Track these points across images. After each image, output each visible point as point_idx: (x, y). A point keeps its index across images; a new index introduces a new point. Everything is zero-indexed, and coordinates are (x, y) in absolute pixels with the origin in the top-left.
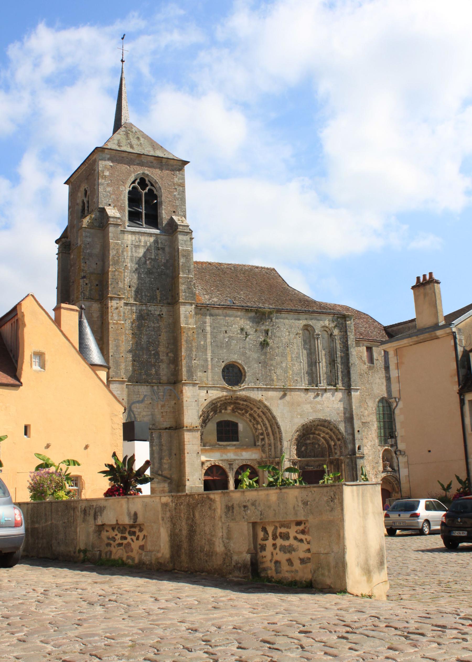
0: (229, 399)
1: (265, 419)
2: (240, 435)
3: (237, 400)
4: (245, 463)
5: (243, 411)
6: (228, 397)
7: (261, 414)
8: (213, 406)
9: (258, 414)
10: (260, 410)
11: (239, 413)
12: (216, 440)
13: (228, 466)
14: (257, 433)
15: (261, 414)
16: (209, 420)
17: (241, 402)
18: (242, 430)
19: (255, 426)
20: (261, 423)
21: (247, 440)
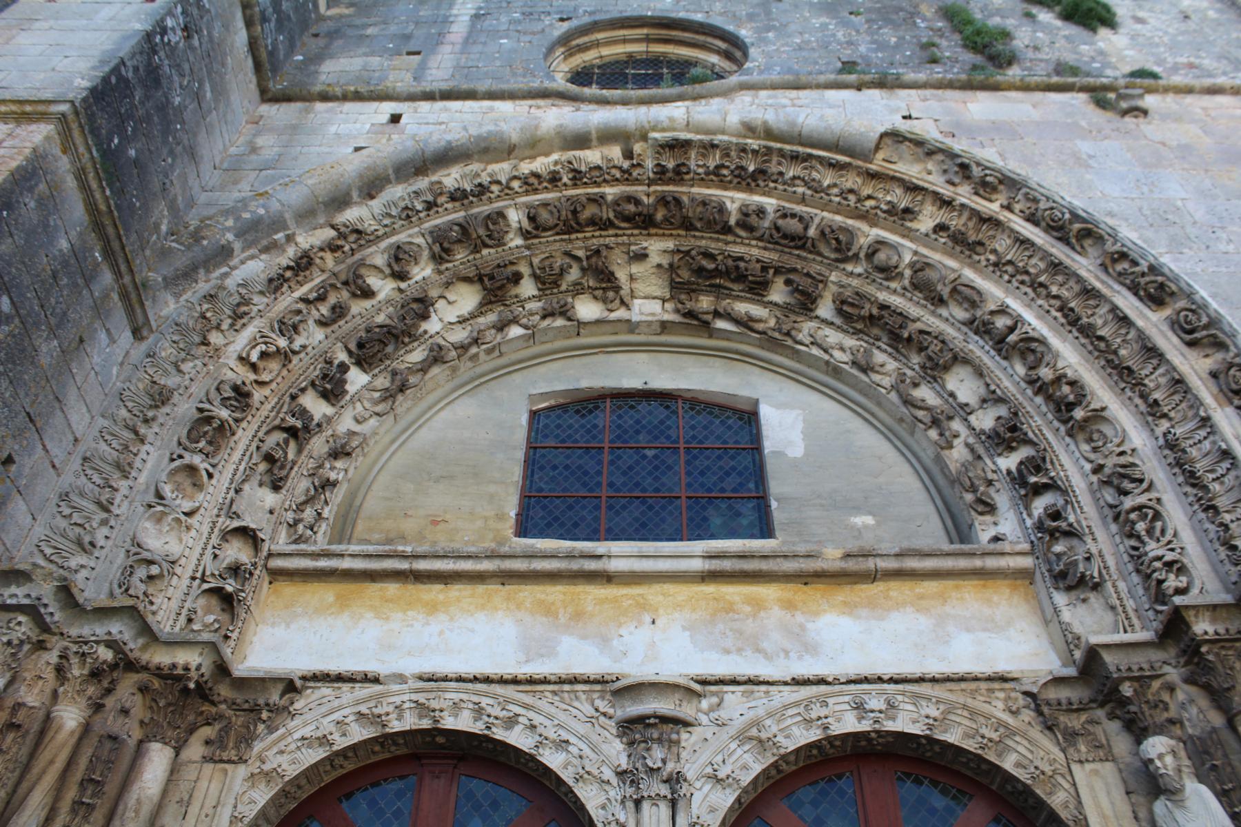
0: (598, 175)
1: (994, 291)
2: (778, 486)
3: (679, 175)
4: (849, 724)
5: (778, 293)
6: (592, 156)
7: (948, 263)
8: (451, 215)
9: (920, 267)
10: (926, 221)
11: (746, 323)
12: (508, 527)
13: (617, 751)
14: (958, 454)
15: (948, 263)
16: (437, 357)
17: (734, 200)
18: (797, 450)
19: (924, 393)
20: (978, 348)
21: (863, 520)
